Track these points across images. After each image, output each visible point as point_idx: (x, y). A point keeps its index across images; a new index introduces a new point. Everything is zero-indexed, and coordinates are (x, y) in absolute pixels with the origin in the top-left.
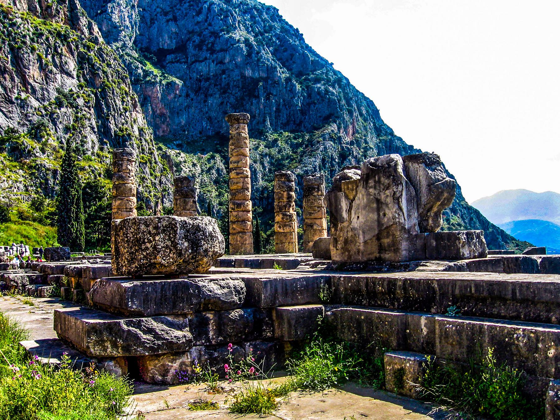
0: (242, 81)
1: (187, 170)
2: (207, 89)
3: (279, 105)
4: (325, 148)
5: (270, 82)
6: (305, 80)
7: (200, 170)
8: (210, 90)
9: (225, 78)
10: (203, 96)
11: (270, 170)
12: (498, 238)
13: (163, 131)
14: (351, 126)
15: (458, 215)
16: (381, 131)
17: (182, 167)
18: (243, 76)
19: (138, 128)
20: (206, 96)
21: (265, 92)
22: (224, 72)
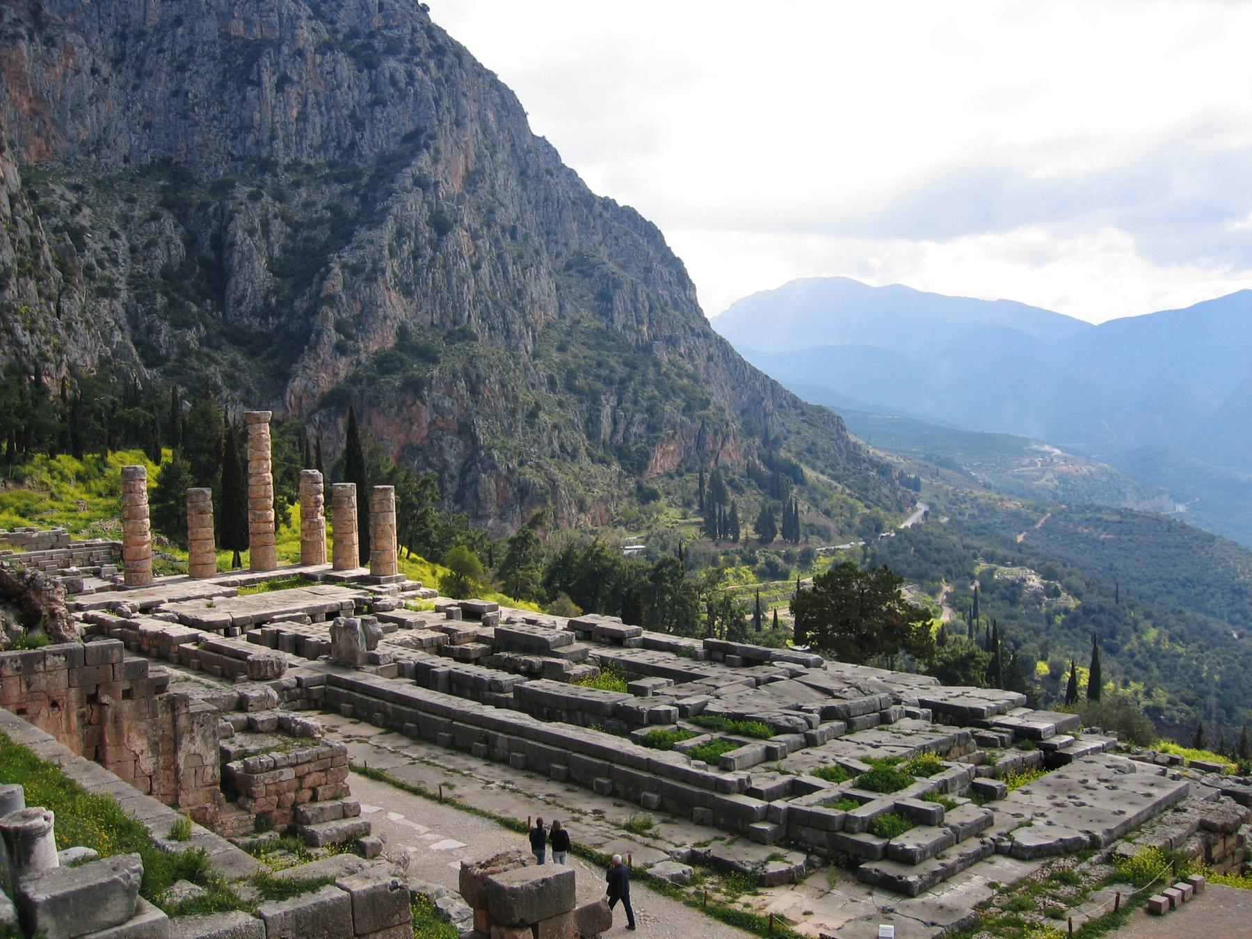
0: (221, 45)
1: (98, 247)
2: (141, 60)
3: (305, 104)
4: (403, 207)
5: (285, 50)
6: (363, 47)
7: (128, 245)
8: (148, 61)
9: (182, 36)
10: (131, 74)
11: (284, 250)
12: (763, 399)
13: (39, 153)
14: (462, 156)
15: (682, 351)
16: (527, 164)
17: (88, 240)
18: (226, 36)
19: (9, 196)
20: (138, 75)
21: (274, 73)
22: (178, 21)
